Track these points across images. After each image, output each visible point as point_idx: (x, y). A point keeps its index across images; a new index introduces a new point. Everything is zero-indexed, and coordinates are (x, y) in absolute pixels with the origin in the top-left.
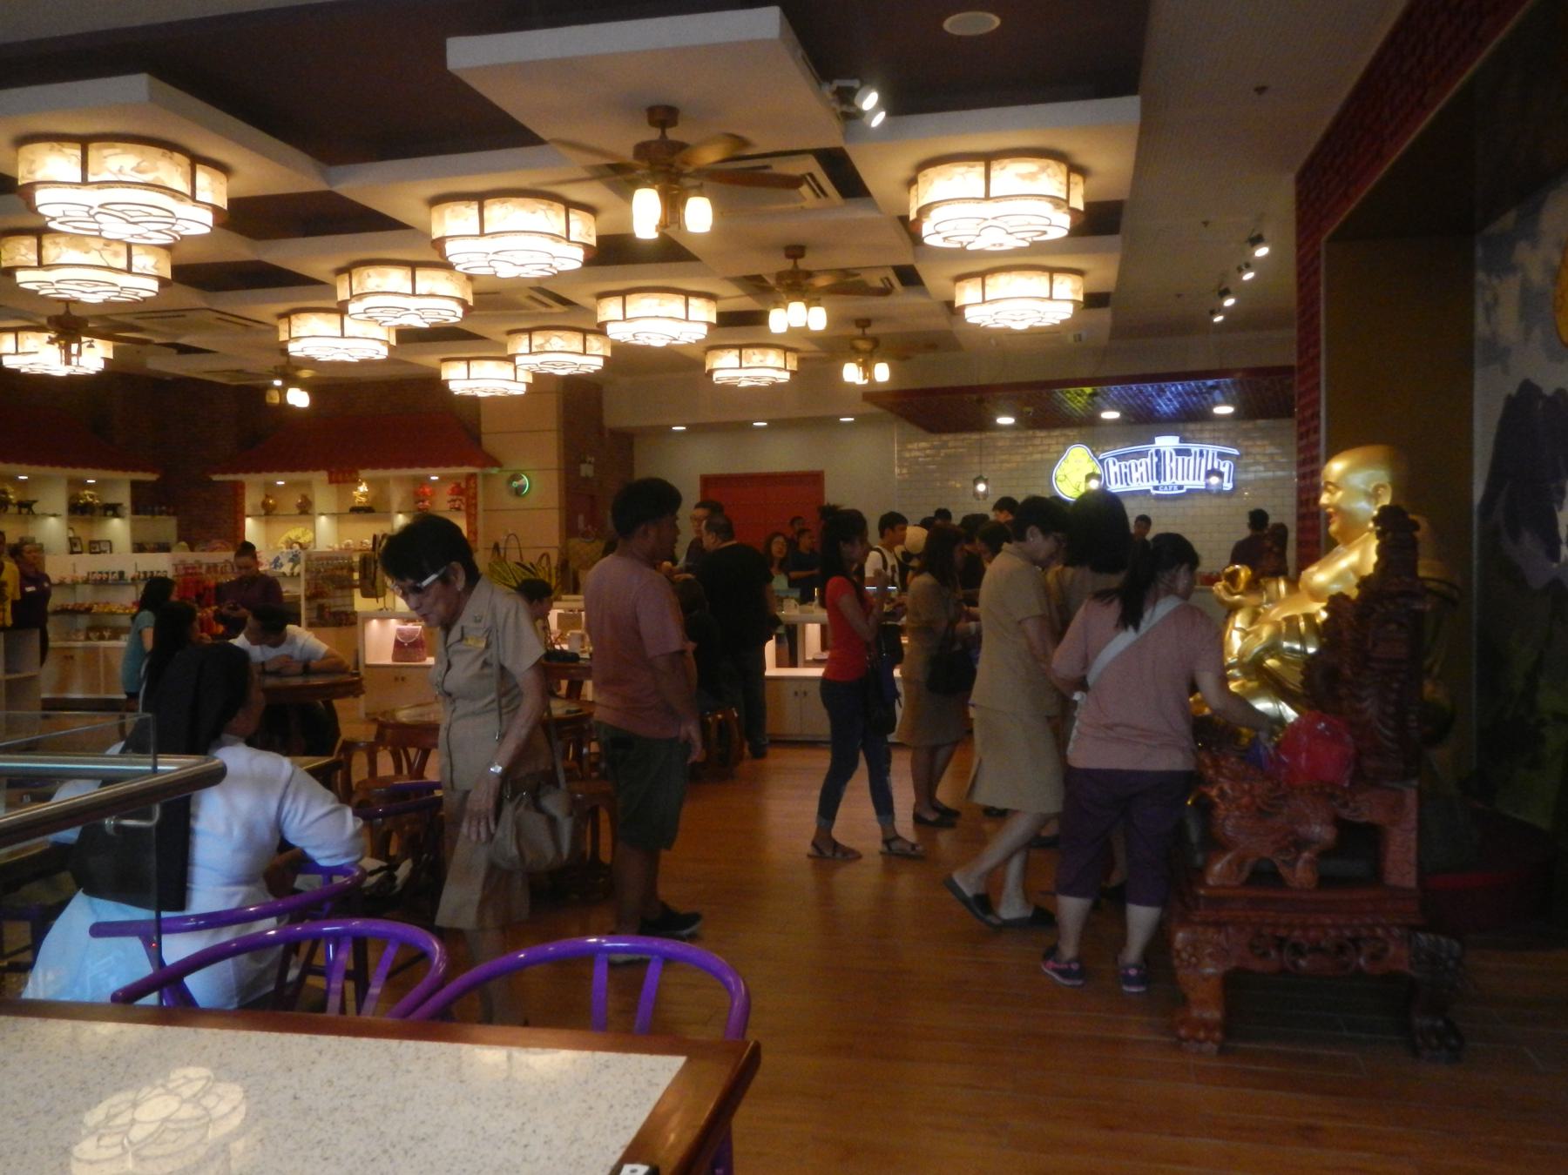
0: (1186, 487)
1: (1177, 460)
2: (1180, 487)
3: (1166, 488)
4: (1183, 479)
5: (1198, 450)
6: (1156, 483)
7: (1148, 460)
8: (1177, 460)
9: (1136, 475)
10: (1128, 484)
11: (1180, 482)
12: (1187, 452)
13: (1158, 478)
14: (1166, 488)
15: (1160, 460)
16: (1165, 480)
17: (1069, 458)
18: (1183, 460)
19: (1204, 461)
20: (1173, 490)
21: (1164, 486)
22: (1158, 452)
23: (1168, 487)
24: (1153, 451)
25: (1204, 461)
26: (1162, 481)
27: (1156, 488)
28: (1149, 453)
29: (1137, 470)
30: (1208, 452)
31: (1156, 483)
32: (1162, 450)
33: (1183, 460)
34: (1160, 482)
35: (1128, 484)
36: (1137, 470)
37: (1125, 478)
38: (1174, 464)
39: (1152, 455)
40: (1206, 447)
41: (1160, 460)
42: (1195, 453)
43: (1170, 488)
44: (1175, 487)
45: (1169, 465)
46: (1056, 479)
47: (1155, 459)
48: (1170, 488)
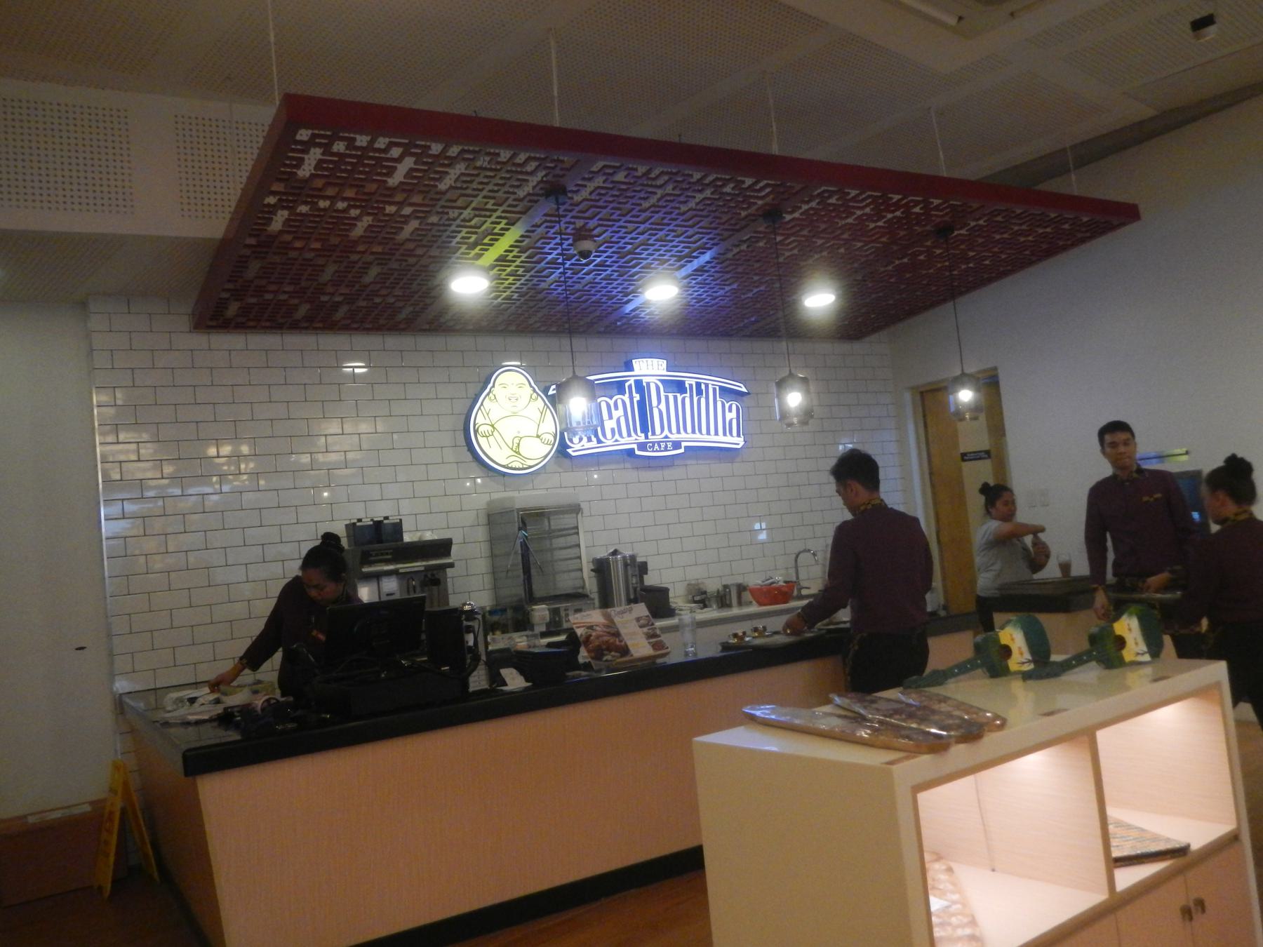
0: (683, 444)
1: (667, 398)
2: (677, 445)
3: (656, 447)
4: (678, 432)
5: (693, 382)
6: (642, 438)
7: (626, 398)
8: (667, 398)
9: (609, 425)
10: (599, 441)
11: (675, 437)
12: (680, 387)
13: (645, 429)
14: (656, 447)
15: (643, 398)
16: (654, 434)
17: (496, 390)
18: (675, 398)
19: (703, 401)
20: (666, 450)
21: (653, 443)
22: (639, 384)
23: (659, 443)
24: (632, 381)
25: (703, 401)
26: (650, 434)
27: (642, 446)
28: (627, 385)
29: (611, 417)
30: (707, 386)
31: (642, 438)
32: (645, 380)
33: (675, 398)
34: (647, 437)
35: (599, 441)
36: (611, 417)
37: (594, 429)
38: (663, 406)
39: (630, 387)
40: (705, 379)
41: (643, 398)
42: (691, 386)
43: (663, 445)
44: (669, 445)
45: (658, 408)
46: (476, 431)
47: (637, 397)
48: (663, 445)
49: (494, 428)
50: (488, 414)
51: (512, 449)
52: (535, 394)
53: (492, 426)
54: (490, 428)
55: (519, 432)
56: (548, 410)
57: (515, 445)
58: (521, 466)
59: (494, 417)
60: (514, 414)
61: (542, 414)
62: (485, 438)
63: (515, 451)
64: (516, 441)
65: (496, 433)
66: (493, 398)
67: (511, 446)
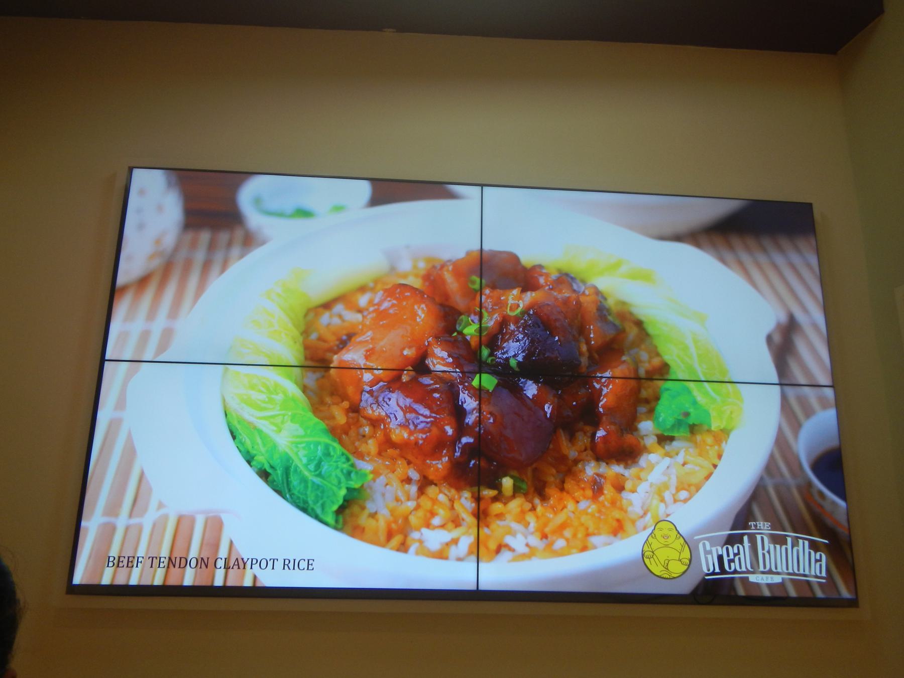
49: (654, 553)
50: (650, 546)
51: (664, 567)
52: (679, 535)
53: (653, 552)
54: (651, 554)
55: (668, 557)
56: (686, 545)
57: (666, 564)
58: (669, 577)
59: (654, 547)
60: (667, 546)
61: (682, 546)
62: (648, 559)
63: (665, 568)
64: (667, 562)
65: (654, 557)
66: (654, 536)
67: (663, 564)
